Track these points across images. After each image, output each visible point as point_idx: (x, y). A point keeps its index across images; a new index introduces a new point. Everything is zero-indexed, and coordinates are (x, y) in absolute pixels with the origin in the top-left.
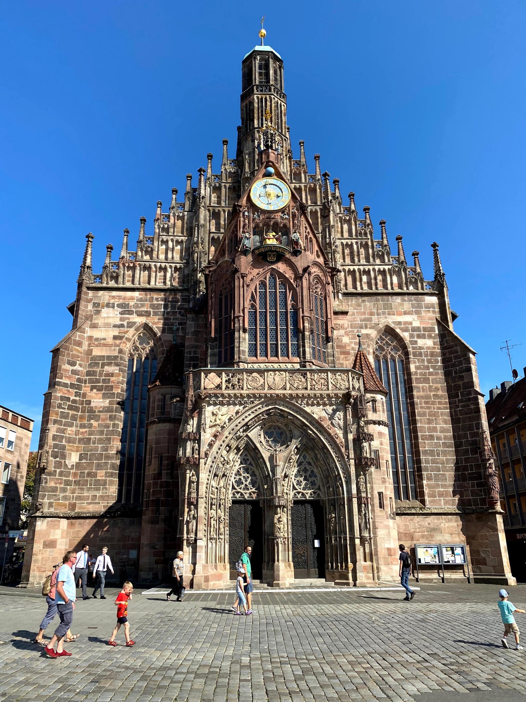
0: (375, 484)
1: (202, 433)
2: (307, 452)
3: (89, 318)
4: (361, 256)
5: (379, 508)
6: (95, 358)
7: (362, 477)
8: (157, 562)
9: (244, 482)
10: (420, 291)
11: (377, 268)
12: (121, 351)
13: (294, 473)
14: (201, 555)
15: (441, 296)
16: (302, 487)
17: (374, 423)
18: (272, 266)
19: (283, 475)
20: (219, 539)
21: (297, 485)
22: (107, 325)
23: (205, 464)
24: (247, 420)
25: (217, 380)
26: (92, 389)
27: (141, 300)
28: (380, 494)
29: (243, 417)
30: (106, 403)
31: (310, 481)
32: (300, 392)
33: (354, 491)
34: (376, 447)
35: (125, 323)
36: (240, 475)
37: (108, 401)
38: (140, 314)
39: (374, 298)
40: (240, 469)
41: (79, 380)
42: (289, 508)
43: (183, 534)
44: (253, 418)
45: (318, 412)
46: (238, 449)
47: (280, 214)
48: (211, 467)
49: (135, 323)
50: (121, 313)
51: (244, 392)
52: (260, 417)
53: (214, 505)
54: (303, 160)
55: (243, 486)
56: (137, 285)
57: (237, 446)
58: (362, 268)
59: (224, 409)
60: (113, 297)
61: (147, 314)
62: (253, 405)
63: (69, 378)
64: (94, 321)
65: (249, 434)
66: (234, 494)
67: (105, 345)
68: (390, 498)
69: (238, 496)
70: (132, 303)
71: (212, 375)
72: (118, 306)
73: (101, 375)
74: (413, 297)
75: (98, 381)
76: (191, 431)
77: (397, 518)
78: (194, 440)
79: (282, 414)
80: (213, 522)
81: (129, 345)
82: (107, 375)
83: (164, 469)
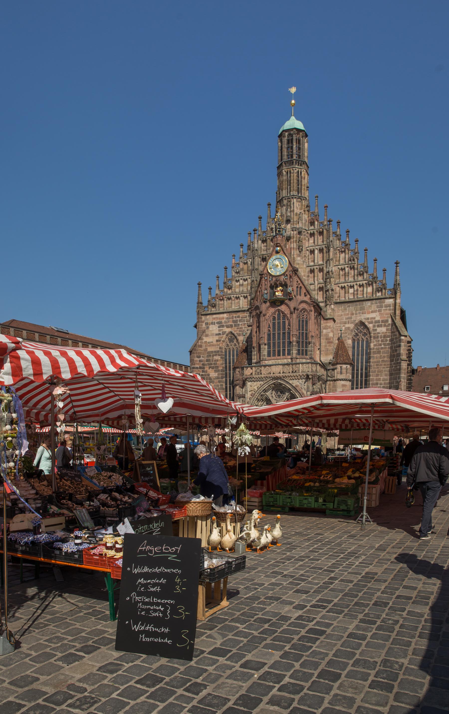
3: (204, 332)
4: (350, 276)
6: (209, 352)
10: (384, 296)
11: (358, 283)
12: (220, 348)
15: (395, 298)
17: (340, 380)
18: (279, 308)
22: (212, 335)
25: (251, 371)
26: (210, 368)
27: (227, 318)
30: (216, 375)
32: (287, 375)
35: (221, 332)
37: (217, 374)
38: (228, 327)
39: (355, 304)
41: (203, 364)
45: (295, 383)
47: (283, 277)
49: (225, 332)
50: (219, 327)
51: (263, 376)
54: (316, 211)
56: (225, 311)
58: (349, 284)
59: (255, 383)
60: (214, 318)
61: (231, 326)
63: (198, 364)
64: (207, 333)
67: (213, 345)
70: (223, 321)
71: (249, 368)
72: (217, 323)
73: (212, 361)
74: (378, 301)
75: (211, 364)
79: (281, 384)
81: (224, 344)
82: (215, 361)
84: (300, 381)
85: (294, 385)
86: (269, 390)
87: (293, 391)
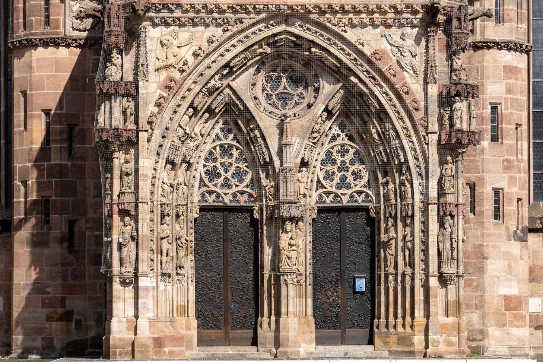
0: (488, 172)
1: (141, 83)
2: (348, 117)
5: (492, 220)
7: (450, 166)
8: (49, 319)
9: (222, 172)
13: (320, 158)
14: (147, 302)
16: (334, 183)
19: (299, 161)
20: (177, 275)
21: (325, 178)
23: (149, 141)
24: (228, 56)
28: (496, 191)
29: (221, 50)
31: (351, 170)
33: (433, 193)
34: (496, 98)
36: (215, 160)
40: (215, 148)
42: (309, 220)
43: (110, 265)
44: (242, 52)
45: (371, 40)
46: (211, 111)
48: (161, 146)
52: (255, 50)
53: (168, 215)
55: (220, 181)
57: (210, 106)
59: (184, 34)
62: (240, 27)
65: (234, 84)
66: (203, 195)
68: (519, 200)
69: (211, 199)
76: (118, 77)
77: (531, 237)
78: (127, 94)
79: (300, 44)
80: (165, 245)
83: (55, 141)
84: (395, 33)
85: (367, 50)
86: (244, 67)
87: (362, 77)
